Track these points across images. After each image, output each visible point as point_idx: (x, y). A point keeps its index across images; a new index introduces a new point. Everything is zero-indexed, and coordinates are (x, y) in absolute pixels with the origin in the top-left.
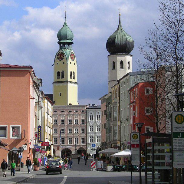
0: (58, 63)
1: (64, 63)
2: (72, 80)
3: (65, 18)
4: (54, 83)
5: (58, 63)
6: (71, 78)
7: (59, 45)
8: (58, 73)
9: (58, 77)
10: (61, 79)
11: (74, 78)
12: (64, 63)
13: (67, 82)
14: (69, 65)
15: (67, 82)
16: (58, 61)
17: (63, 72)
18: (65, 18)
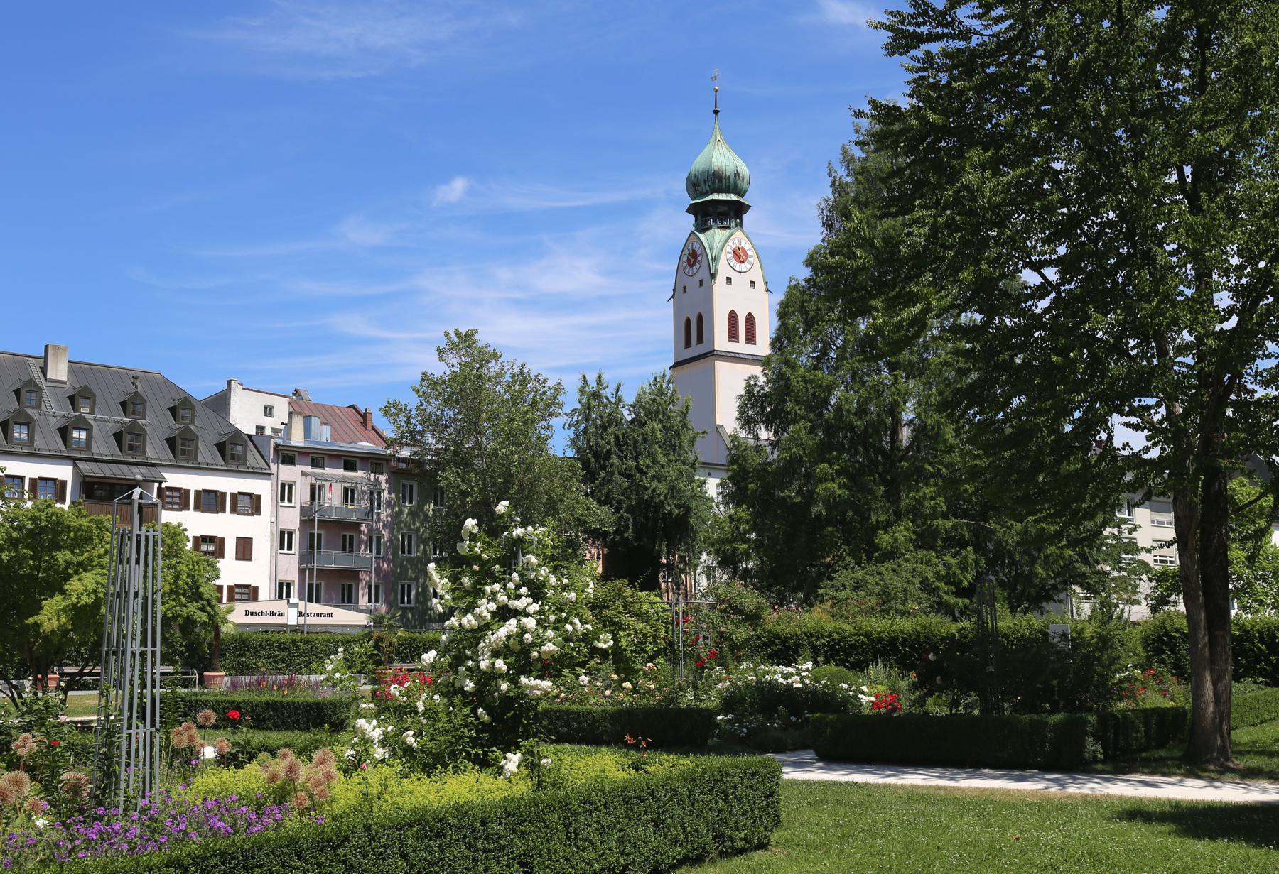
0: (685, 288)
1: (701, 282)
2: (742, 347)
3: (716, 112)
4: (677, 365)
5: (685, 288)
6: (733, 336)
7: (692, 218)
8: (688, 322)
9: (688, 344)
10: (695, 350)
11: (751, 338)
12: (701, 282)
13: (711, 354)
14: (719, 286)
15: (711, 354)
18: (716, 112)
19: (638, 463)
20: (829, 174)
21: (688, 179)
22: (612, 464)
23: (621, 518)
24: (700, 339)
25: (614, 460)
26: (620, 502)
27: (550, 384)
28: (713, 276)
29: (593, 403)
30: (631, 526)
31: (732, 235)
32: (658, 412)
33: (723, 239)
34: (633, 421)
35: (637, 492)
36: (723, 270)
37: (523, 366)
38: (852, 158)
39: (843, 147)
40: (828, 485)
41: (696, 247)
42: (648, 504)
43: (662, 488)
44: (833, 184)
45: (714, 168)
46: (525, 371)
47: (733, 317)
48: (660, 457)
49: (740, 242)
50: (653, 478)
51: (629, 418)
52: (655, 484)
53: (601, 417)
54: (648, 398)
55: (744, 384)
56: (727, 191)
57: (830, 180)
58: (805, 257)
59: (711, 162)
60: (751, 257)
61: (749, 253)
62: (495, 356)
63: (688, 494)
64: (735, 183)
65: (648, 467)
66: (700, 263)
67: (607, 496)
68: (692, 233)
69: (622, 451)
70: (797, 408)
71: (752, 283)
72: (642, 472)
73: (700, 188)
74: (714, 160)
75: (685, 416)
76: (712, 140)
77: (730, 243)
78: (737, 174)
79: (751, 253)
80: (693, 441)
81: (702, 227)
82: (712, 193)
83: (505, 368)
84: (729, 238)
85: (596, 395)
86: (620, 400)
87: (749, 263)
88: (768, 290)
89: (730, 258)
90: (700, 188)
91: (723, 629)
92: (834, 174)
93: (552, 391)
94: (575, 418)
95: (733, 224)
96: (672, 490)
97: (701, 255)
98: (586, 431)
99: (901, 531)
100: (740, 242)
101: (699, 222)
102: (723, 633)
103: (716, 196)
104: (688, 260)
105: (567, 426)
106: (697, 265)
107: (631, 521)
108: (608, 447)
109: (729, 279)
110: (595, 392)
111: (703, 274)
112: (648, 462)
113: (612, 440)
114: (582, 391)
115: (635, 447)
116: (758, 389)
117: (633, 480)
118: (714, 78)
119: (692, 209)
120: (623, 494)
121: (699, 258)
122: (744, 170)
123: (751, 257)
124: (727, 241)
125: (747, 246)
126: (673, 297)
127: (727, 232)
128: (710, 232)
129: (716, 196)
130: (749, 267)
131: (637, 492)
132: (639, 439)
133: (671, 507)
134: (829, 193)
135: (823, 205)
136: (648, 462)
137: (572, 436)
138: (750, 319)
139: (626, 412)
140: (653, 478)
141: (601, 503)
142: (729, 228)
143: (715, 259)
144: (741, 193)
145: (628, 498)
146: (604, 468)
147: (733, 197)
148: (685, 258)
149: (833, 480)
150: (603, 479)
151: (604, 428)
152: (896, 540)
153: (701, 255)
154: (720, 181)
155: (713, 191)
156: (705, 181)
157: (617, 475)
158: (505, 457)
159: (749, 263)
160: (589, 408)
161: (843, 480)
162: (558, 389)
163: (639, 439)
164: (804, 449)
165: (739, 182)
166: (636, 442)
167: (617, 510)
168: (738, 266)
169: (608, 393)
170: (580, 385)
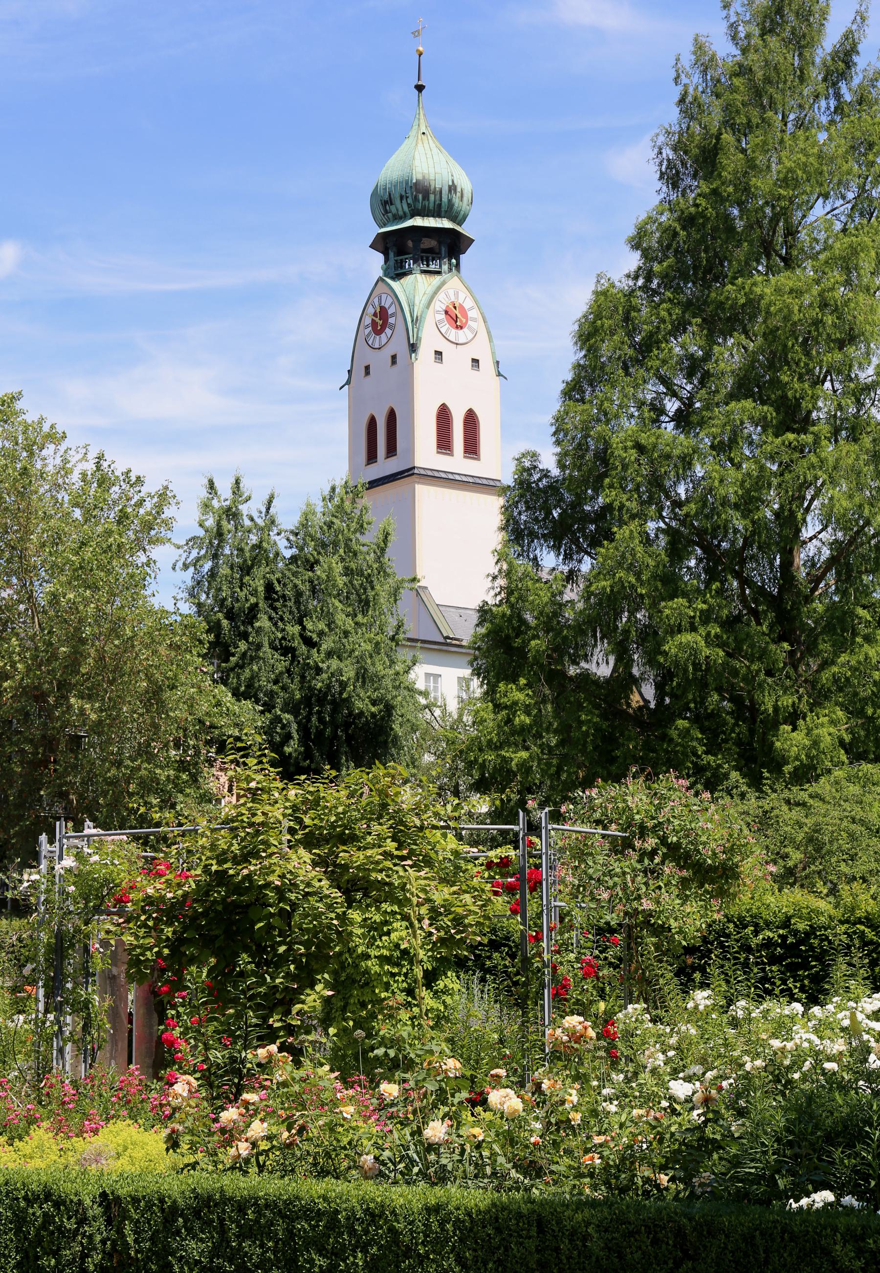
0: (367, 368)
1: (394, 358)
3: (420, 88)
5: (367, 368)
6: (444, 444)
7: (379, 258)
8: (372, 423)
9: (372, 457)
10: (385, 466)
11: (472, 448)
12: (394, 358)
13: (408, 473)
14: (424, 359)
15: (408, 473)
16: (369, 357)
17: (392, 417)
18: (420, 88)
19: (304, 628)
20: (677, 80)
21: (375, 194)
22: (259, 631)
23: (278, 719)
24: (391, 450)
25: (263, 622)
26: (271, 694)
27: (151, 487)
28: (413, 348)
29: (228, 526)
30: (296, 736)
31: (443, 283)
32: (335, 544)
33: (430, 290)
34: (294, 559)
35: (303, 677)
36: (429, 340)
37: (100, 458)
38: (713, 58)
39: (696, 40)
40: (686, 638)
41: (387, 302)
42: (322, 697)
43: (349, 672)
44: (682, 101)
45: (417, 176)
46: (105, 465)
47: (444, 416)
48: (340, 618)
49: (457, 294)
50: (329, 654)
51: (288, 553)
52: (334, 663)
53: (241, 550)
54: (319, 519)
55: (512, 467)
56: (437, 213)
57: (676, 92)
58: (632, 231)
59: (411, 167)
60: (474, 320)
61: (471, 314)
62: (55, 437)
63: (387, 682)
64: (450, 201)
65: (321, 634)
66: (393, 327)
67: (249, 686)
68: (380, 279)
69: (275, 609)
70: (625, 497)
71: (475, 361)
72: (309, 643)
73: (393, 208)
74: (417, 163)
75: (383, 550)
76: (413, 133)
77: (441, 296)
78: (452, 188)
79: (473, 314)
80: (395, 594)
81: (397, 272)
82: (412, 216)
83: (73, 461)
84: (439, 288)
85: (231, 513)
86: (273, 522)
87: (470, 328)
88: (499, 374)
89: (441, 321)
90: (393, 208)
91: (647, 905)
92: (684, 80)
93: (156, 500)
94: (194, 553)
95: (445, 267)
96: (363, 676)
97: (393, 315)
98: (213, 574)
99: (822, 725)
100: (457, 294)
101: (392, 262)
102: (650, 914)
103: (418, 222)
104: (374, 324)
105: (180, 565)
106: (388, 331)
107: (294, 726)
108: (253, 600)
109: (439, 354)
110: (229, 509)
111: (398, 345)
112: (321, 626)
113: (261, 589)
114: (206, 506)
115: (298, 602)
116: (536, 477)
117: (294, 657)
118: (416, 34)
119: (383, 243)
120: (276, 682)
121: (391, 320)
122: (464, 183)
123: (474, 320)
124: (435, 293)
125: (468, 304)
126: (348, 382)
127: (436, 280)
128: (408, 280)
129: (418, 222)
130: (470, 336)
131: (303, 677)
132: (305, 588)
133: (362, 704)
134: (672, 116)
135: (662, 139)
136: (321, 626)
137: (190, 583)
138: (471, 420)
139: (282, 543)
140: (329, 654)
141: (237, 695)
142: (439, 273)
143: (416, 321)
144: (458, 218)
145: (284, 688)
146: (245, 636)
147: (446, 224)
148: (368, 320)
149: (693, 629)
150: (244, 655)
151: (246, 570)
152: (816, 743)
153: (393, 315)
154: (426, 197)
155: (414, 214)
156: (401, 197)
157: (266, 648)
158: (73, 607)
159: (470, 328)
160: (220, 534)
161: (715, 629)
162: (163, 497)
163: (305, 588)
164: (638, 575)
165: (456, 200)
166: (299, 594)
167: (268, 707)
168: (453, 334)
169: (251, 509)
170: (204, 493)
